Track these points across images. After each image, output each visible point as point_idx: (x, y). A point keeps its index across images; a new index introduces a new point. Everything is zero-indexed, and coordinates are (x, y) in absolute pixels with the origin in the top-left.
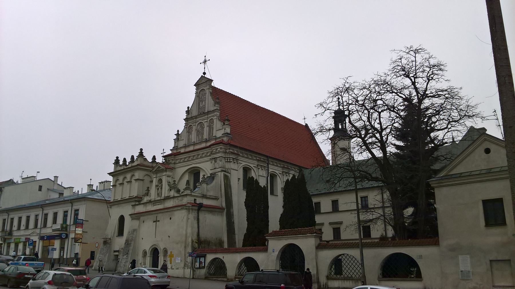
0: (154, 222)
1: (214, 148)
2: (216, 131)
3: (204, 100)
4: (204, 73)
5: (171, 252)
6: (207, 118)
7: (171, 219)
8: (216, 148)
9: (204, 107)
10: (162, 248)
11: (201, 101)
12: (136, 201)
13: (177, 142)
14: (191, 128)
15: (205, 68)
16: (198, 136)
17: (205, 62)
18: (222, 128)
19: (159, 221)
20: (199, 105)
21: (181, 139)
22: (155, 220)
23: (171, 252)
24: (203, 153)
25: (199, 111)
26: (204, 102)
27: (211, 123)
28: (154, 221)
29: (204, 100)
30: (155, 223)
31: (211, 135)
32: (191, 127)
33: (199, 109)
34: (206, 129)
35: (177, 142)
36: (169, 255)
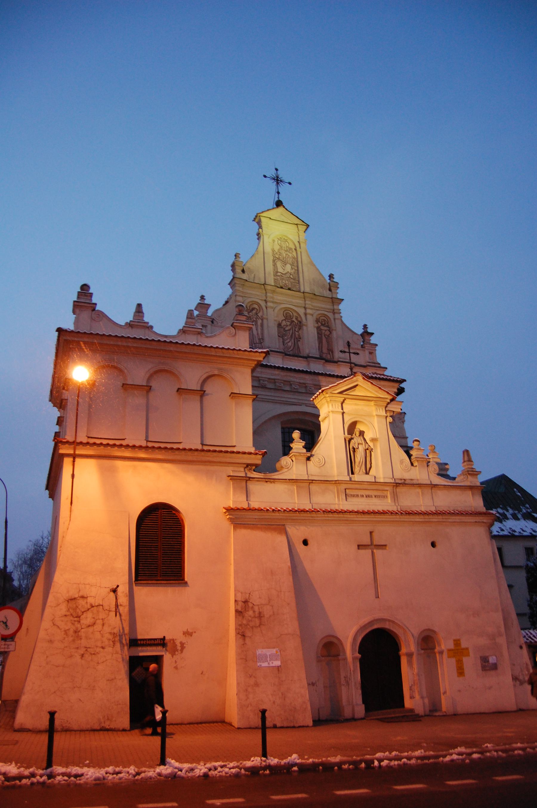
0: (359, 547)
3: (290, 261)
5: (457, 643)
6: (311, 307)
7: (433, 545)
10: (416, 632)
11: (279, 259)
13: (209, 327)
14: (253, 309)
15: (278, 193)
16: (281, 340)
19: (385, 545)
22: (366, 540)
23: (457, 643)
25: (274, 279)
27: (320, 324)
28: (358, 546)
30: (367, 553)
33: (274, 276)
35: (209, 327)
36: (449, 650)
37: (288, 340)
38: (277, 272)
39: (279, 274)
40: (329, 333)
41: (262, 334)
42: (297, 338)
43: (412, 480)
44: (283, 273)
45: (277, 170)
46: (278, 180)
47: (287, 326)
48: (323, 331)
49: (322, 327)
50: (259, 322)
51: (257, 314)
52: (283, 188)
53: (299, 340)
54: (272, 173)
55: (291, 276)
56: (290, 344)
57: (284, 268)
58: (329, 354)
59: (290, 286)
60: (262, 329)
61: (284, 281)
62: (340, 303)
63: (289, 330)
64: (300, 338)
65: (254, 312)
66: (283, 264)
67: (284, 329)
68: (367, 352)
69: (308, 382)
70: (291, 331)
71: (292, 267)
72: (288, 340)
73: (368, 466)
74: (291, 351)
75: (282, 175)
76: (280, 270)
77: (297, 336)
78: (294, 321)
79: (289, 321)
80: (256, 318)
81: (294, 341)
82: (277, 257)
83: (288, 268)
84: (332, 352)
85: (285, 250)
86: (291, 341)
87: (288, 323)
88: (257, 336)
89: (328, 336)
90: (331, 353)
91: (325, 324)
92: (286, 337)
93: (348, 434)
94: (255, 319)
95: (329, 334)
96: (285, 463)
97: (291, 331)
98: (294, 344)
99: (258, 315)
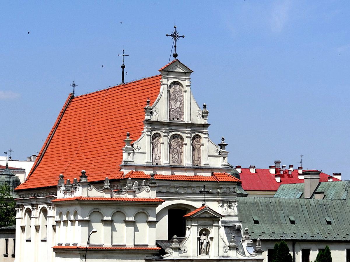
1: (224, 186)
2: (208, 156)
3: (179, 99)
4: (175, 56)
8: (228, 186)
9: (179, 111)
11: (173, 99)
12: (154, 255)
13: (132, 154)
14: (156, 137)
15: (175, 47)
17: (175, 36)
18: (217, 154)
20: (169, 104)
21: (139, 151)
24: (196, 187)
26: (178, 103)
29: (179, 99)
31: (196, 159)
32: (157, 135)
34: (187, 149)
35: (132, 154)
37: (175, 155)
38: (171, 109)
39: (172, 110)
40: (200, 146)
41: (160, 153)
42: (180, 153)
43: (228, 256)
44: (175, 108)
45: (175, 28)
46: (175, 36)
47: (175, 145)
48: (196, 146)
49: (196, 143)
50: (159, 145)
51: (158, 140)
52: (180, 41)
53: (182, 154)
54: (171, 32)
55: (180, 110)
56: (176, 157)
57: (175, 105)
58: (199, 160)
59: (178, 118)
60: (160, 150)
61: (175, 115)
62: (208, 127)
63: (177, 148)
64: (182, 153)
65: (156, 139)
66: (175, 102)
67: (173, 147)
68: (222, 158)
69: (185, 185)
70: (177, 148)
71: (180, 103)
72: (175, 155)
73: (208, 250)
74: (176, 161)
75: (180, 32)
76: (173, 107)
77: (180, 152)
78: (179, 141)
79: (177, 142)
80: (157, 143)
81: (179, 155)
82: (172, 97)
83: (178, 103)
84: (201, 159)
85: (177, 92)
86: (177, 156)
87: (177, 143)
88: (157, 155)
89: (199, 148)
90: (199, 159)
91: (198, 140)
92: (174, 153)
93: (199, 236)
94: (157, 144)
95: (200, 148)
96: (169, 251)
97: (177, 148)
98: (179, 157)
99: (159, 141)
